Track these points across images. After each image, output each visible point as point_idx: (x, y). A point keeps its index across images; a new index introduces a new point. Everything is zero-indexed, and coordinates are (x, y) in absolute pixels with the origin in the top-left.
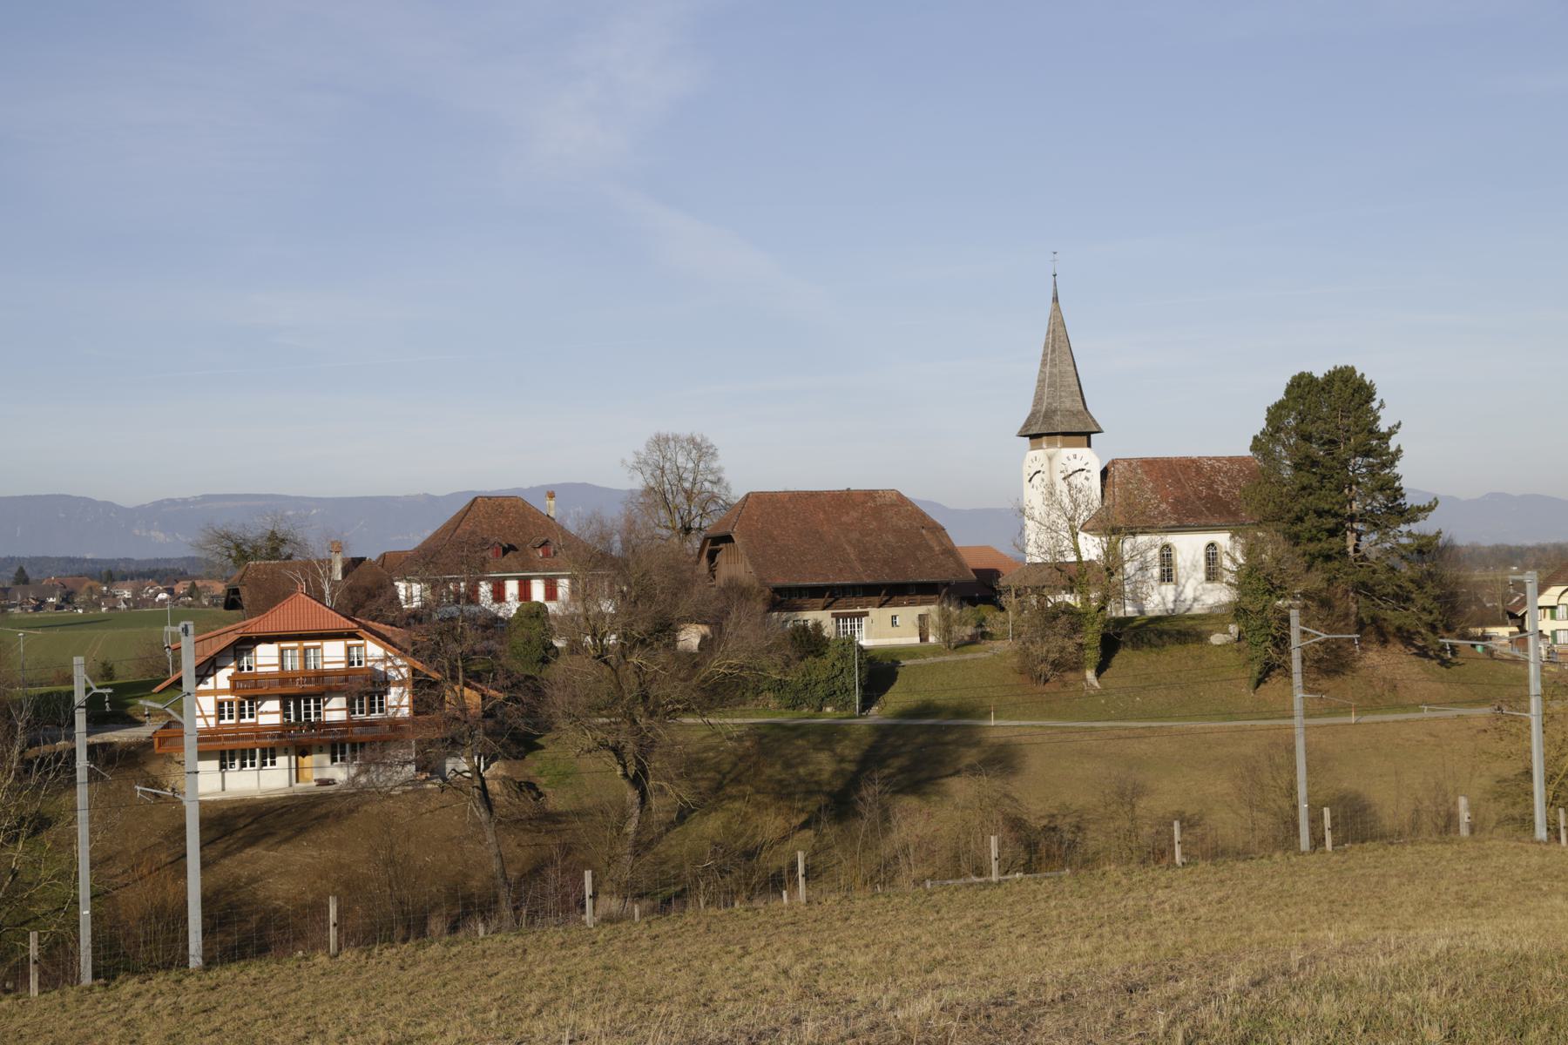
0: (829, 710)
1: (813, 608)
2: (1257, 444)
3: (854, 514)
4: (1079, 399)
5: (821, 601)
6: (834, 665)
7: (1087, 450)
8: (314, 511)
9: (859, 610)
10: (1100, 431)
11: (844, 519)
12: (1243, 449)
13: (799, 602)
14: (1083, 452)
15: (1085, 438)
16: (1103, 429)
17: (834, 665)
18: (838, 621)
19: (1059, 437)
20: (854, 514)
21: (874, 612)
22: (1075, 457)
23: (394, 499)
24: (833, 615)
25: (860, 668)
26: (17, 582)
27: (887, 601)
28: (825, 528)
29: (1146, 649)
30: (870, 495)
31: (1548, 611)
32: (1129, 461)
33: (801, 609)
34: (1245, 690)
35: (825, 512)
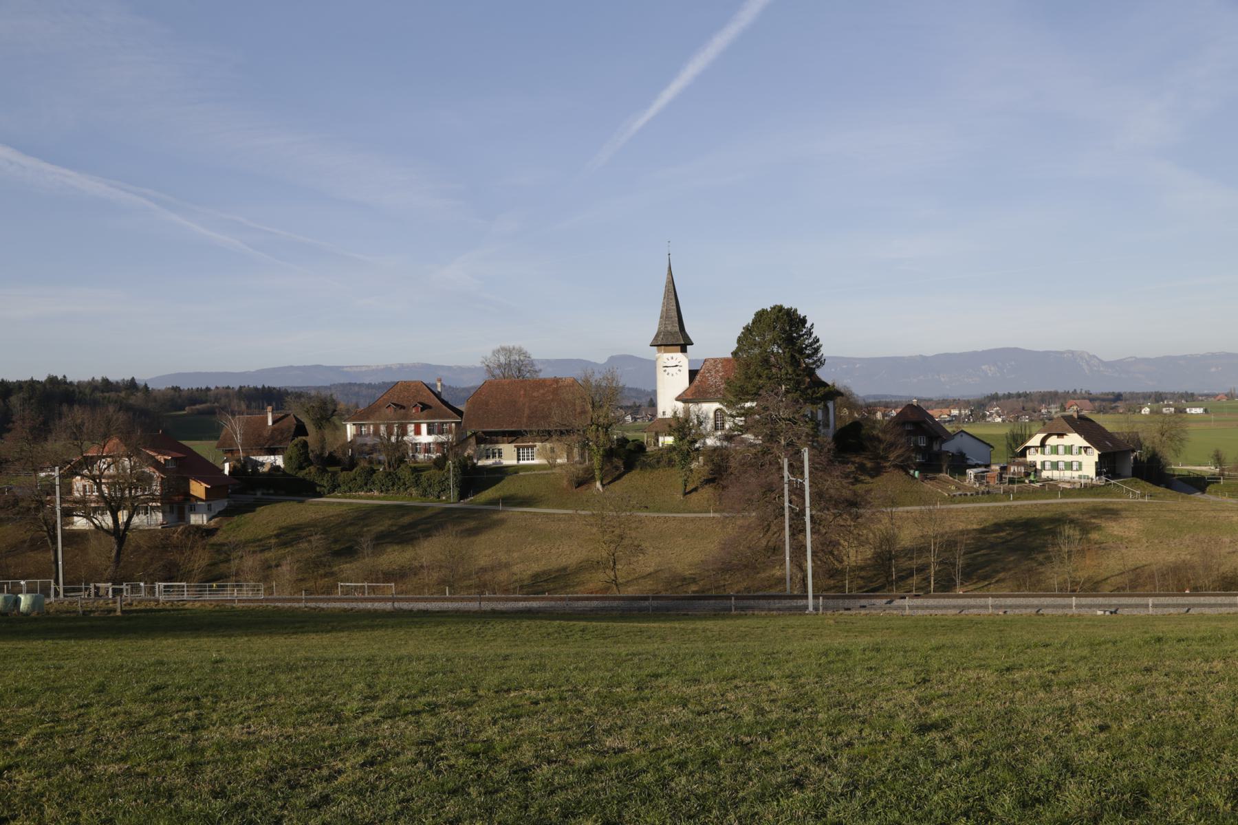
0: (444, 498)
1: (503, 443)
2: (735, 354)
3: (542, 391)
4: (677, 325)
5: (510, 439)
6: (443, 475)
7: (680, 354)
8: (858, 365)
9: (531, 444)
10: (692, 344)
11: (535, 394)
12: (730, 356)
13: (494, 438)
14: (679, 357)
15: (679, 348)
16: (693, 342)
17: (443, 475)
18: (518, 450)
19: (663, 347)
20: (542, 391)
21: (538, 444)
22: (672, 358)
23: (902, 358)
24: (515, 446)
25: (455, 475)
26: (649, 406)
27: (547, 439)
28: (521, 399)
29: (649, 469)
30: (556, 380)
31: (1039, 449)
32: (715, 360)
33: (497, 442)
34: (680, 496)
35: (525, 390)
